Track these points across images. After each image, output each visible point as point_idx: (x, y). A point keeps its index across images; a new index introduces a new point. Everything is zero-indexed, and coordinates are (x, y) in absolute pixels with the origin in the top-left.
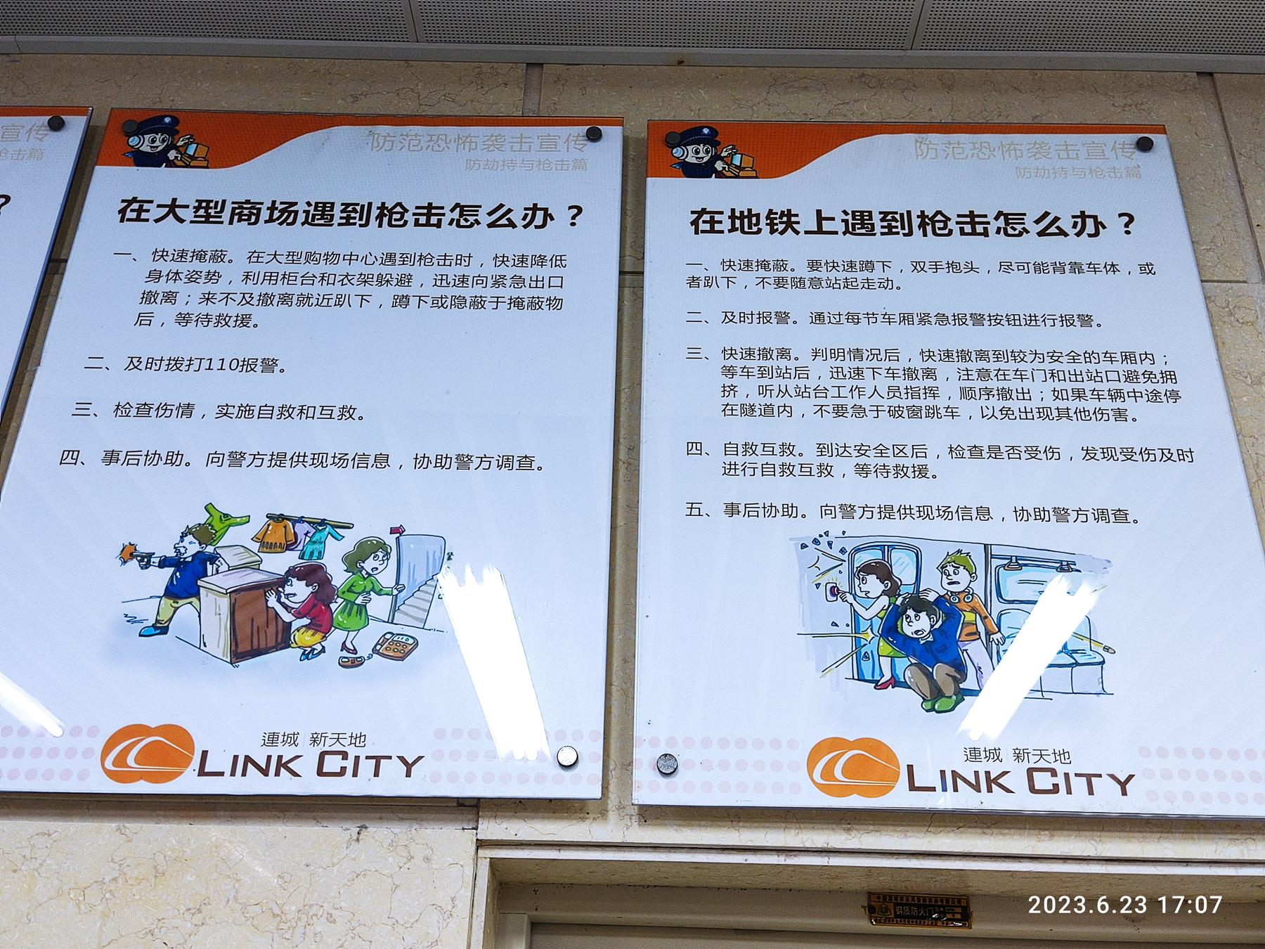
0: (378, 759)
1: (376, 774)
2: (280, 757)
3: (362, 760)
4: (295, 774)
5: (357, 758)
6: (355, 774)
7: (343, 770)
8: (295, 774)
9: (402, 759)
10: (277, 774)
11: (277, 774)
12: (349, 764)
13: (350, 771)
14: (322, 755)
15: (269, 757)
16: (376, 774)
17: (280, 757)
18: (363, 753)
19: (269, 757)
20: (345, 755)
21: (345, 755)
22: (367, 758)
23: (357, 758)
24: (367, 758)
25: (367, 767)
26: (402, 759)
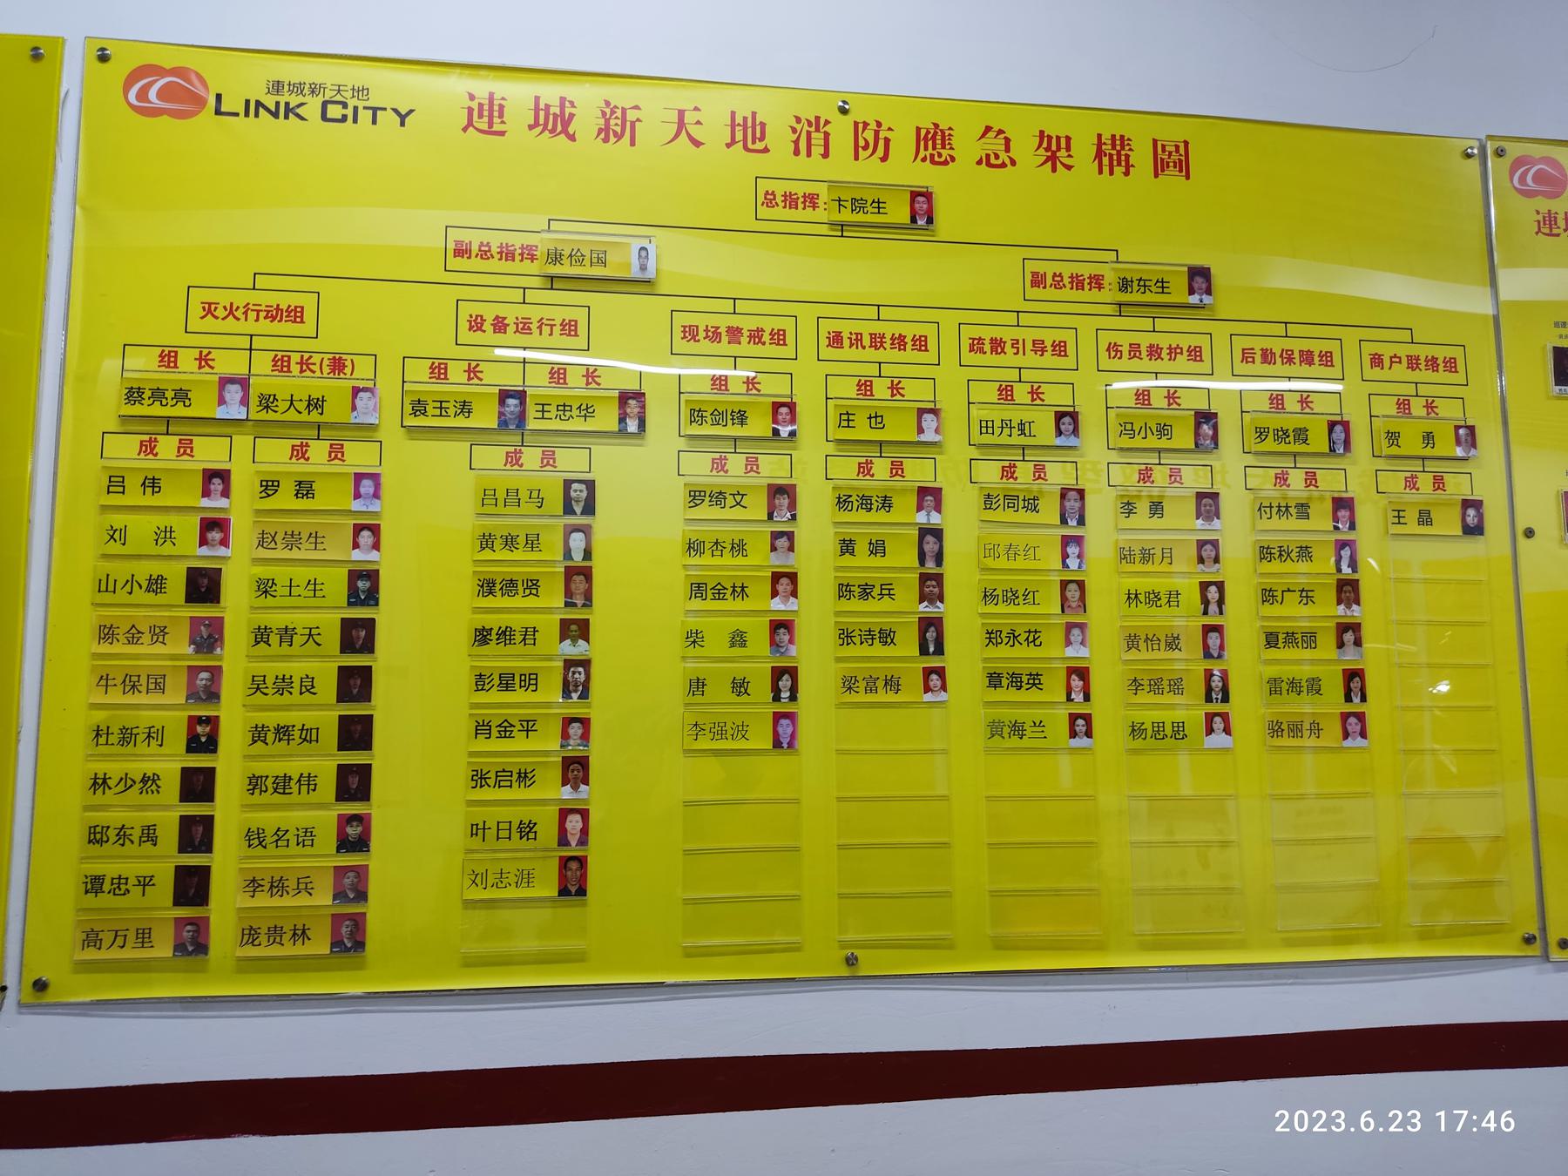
0: (375, 110)
1: (374, 122)
2: (287, 104)
3: (360, 110)
4: (302, 118)
5: (356, 109)
6: (355, 121)
7: (344, 119)
8: (302, 118)
9: (395, 111)
10: (286, 117)
11: (286, 117)
12: (349, 112)
13: (350, 118)
14: (325, 104)
15: (278, 104)
16: (374, 122)
17: (287, 104)
18: (361, 105)
19: (278, 104)
20: (345, 105)
21: (345, 105)
22: (365, 108)
23: (356, 109)
24: (365, 108)
25: (365, 116)
26: (395, 111)
